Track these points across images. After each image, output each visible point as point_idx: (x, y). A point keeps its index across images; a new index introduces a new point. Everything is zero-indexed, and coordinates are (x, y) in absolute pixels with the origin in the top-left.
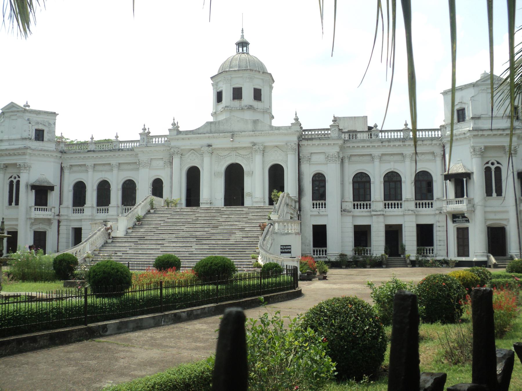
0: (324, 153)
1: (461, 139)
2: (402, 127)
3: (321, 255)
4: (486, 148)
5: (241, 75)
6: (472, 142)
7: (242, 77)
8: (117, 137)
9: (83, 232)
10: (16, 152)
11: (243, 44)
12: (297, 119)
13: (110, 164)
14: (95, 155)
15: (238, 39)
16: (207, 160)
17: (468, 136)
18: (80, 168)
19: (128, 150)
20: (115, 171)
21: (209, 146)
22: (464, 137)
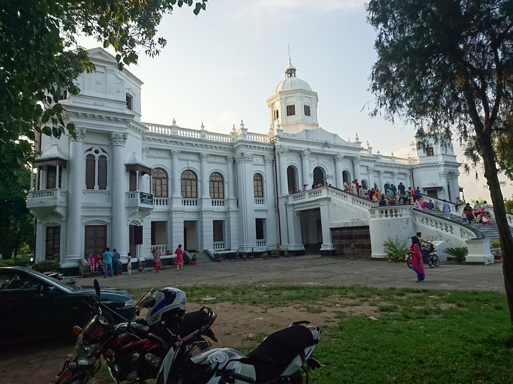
0: (367, 167)
1: (432, 166)
2: (391, 156)
3: (218, 249)
4: (450, 173)
5: (311, 97)
6: (442, 169)
7: (310, 98)
8: (203, 126)
9: (174, 225)
10: (112, 116)
11: (291, 72)
12: (357, 139)
13: (199, 154)
14: (184, 142)
15: (288, 67)
16: (306, 161)
17: (440, 165)
18: (159, 152)
19: (217, 143)
20: (205, 163)
21: (308, 150)
22: (436, 165)
